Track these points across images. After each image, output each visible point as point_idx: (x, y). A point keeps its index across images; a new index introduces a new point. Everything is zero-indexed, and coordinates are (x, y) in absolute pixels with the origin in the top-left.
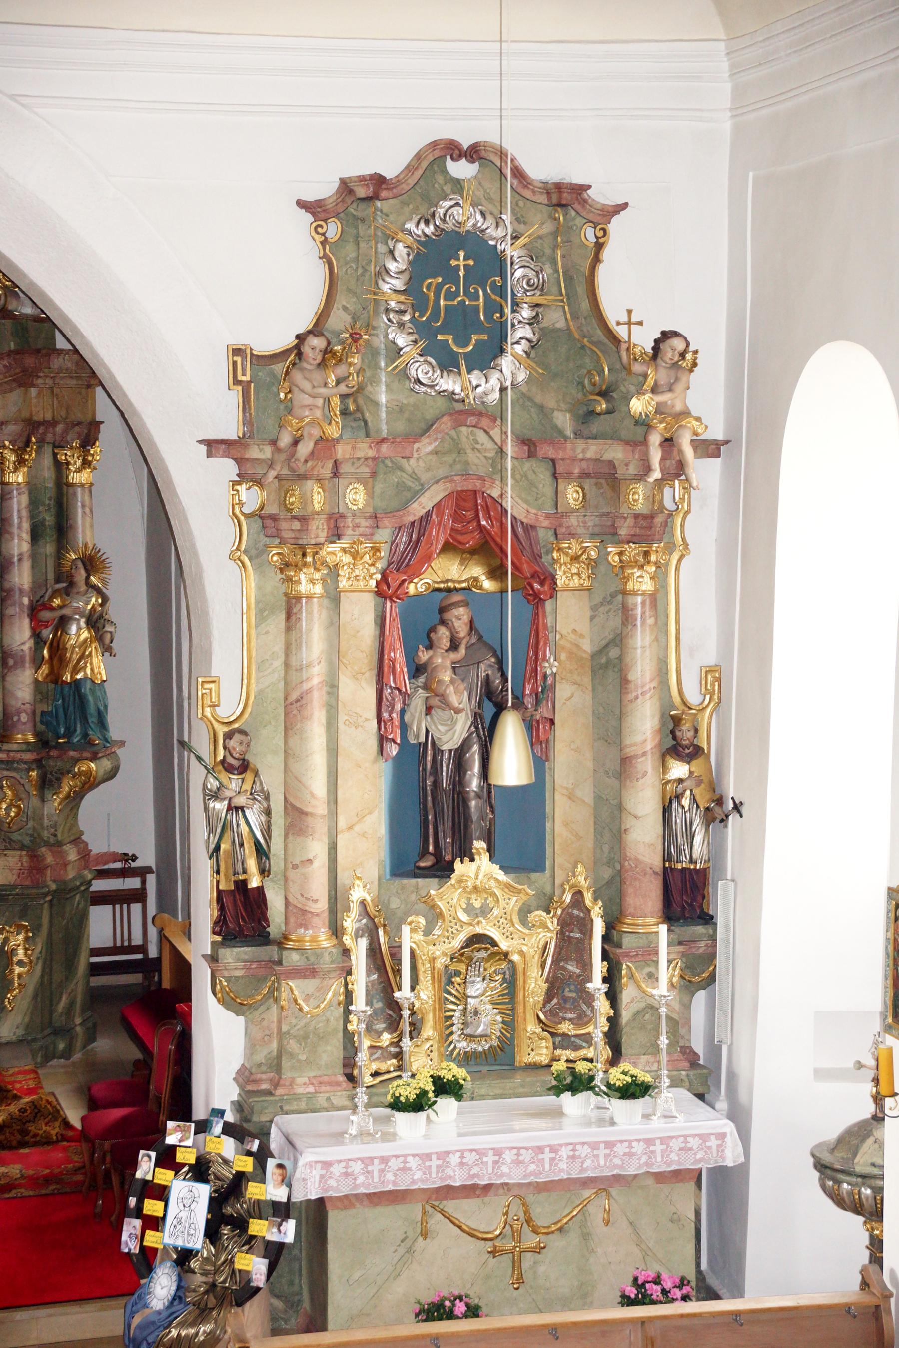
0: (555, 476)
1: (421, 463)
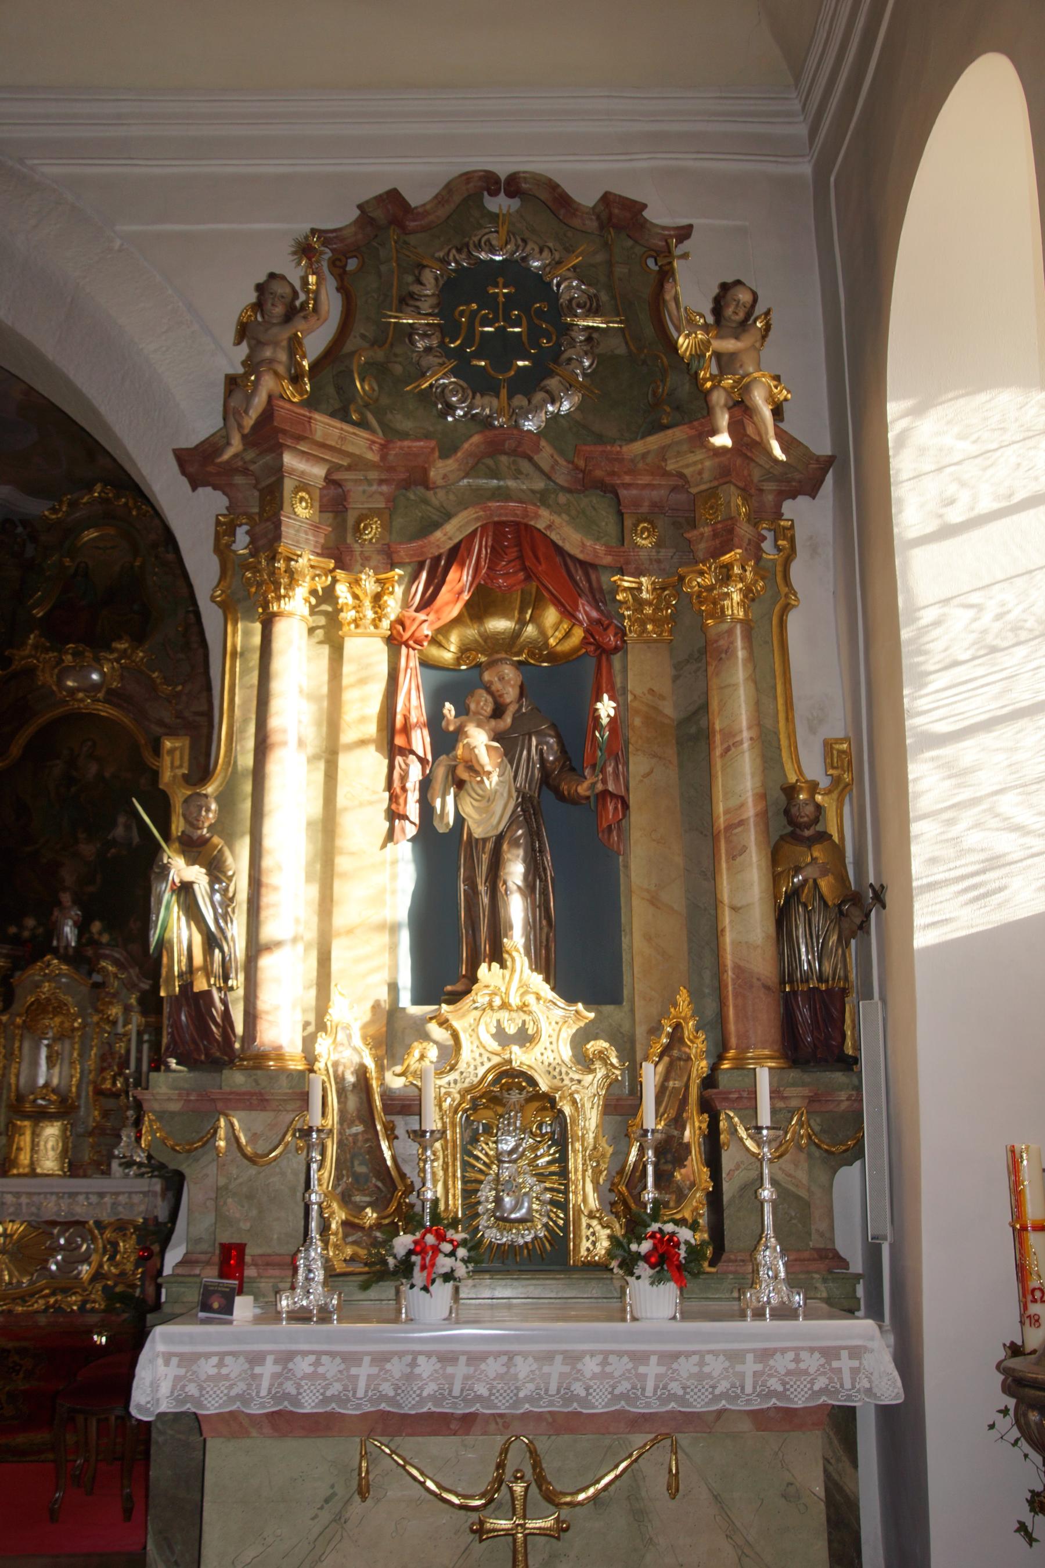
0: (621, 514)
1: (452, 497)
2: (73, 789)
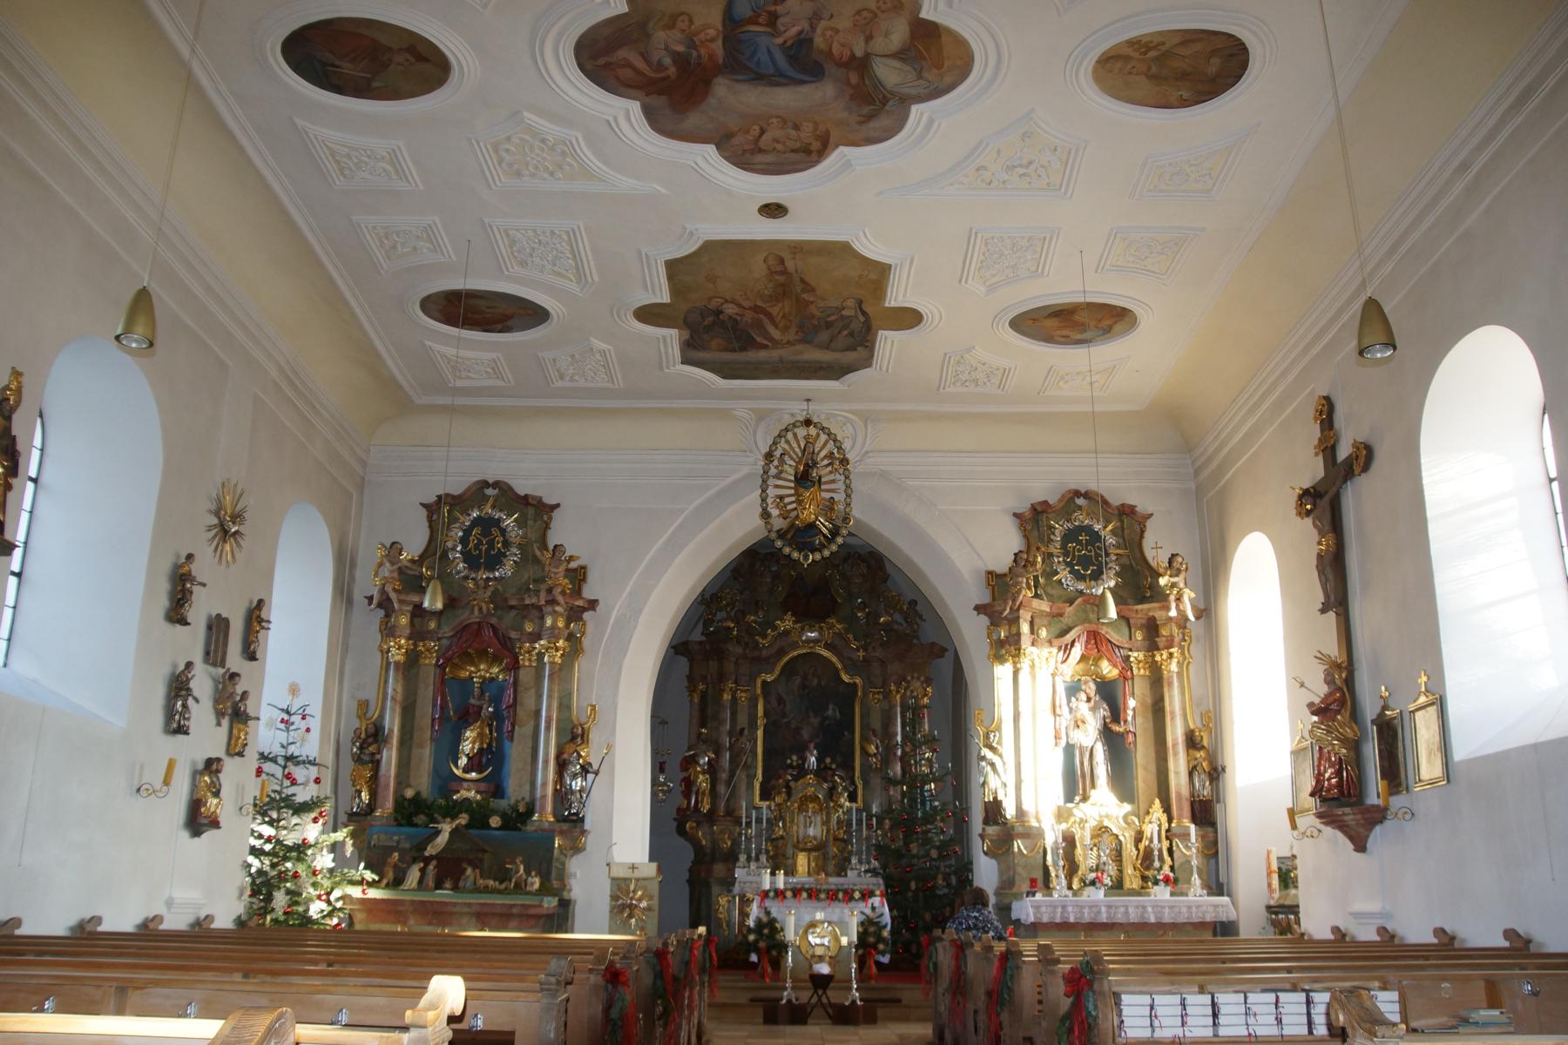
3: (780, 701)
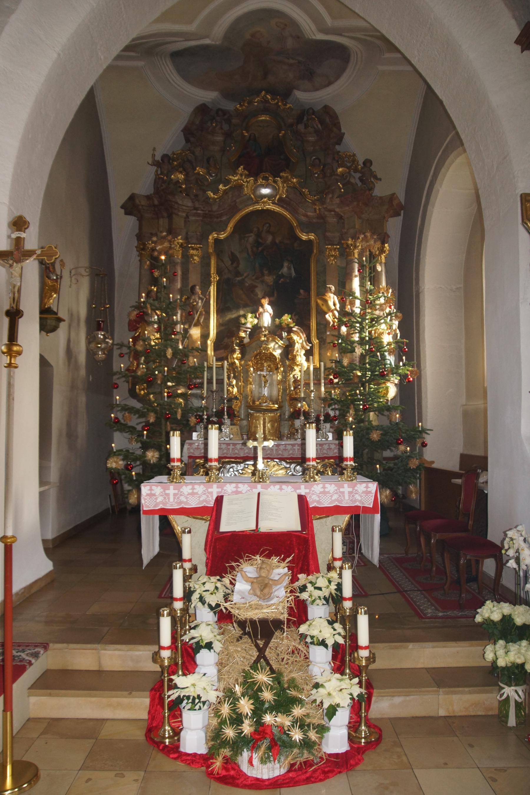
2: (260, 249)
3: (234, 259)
